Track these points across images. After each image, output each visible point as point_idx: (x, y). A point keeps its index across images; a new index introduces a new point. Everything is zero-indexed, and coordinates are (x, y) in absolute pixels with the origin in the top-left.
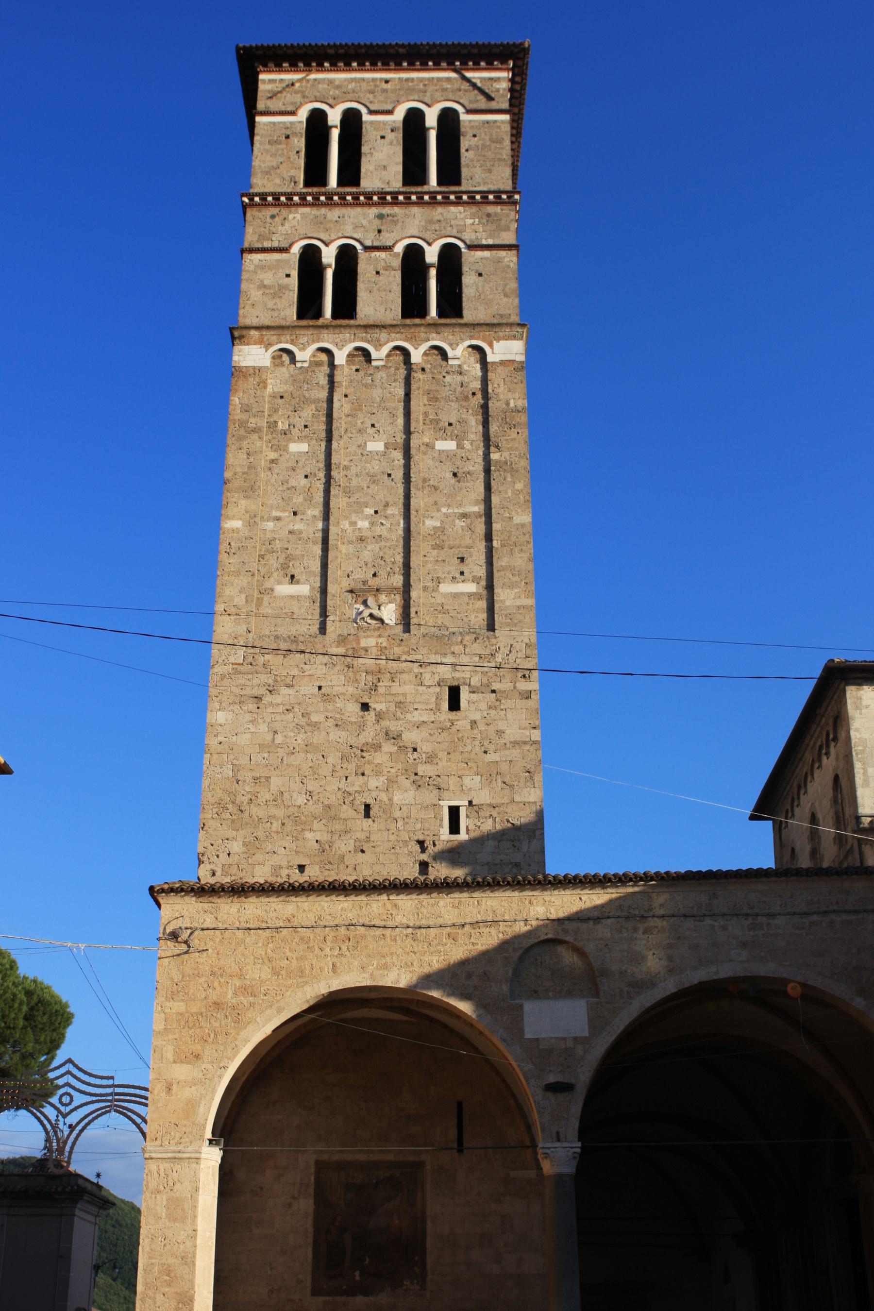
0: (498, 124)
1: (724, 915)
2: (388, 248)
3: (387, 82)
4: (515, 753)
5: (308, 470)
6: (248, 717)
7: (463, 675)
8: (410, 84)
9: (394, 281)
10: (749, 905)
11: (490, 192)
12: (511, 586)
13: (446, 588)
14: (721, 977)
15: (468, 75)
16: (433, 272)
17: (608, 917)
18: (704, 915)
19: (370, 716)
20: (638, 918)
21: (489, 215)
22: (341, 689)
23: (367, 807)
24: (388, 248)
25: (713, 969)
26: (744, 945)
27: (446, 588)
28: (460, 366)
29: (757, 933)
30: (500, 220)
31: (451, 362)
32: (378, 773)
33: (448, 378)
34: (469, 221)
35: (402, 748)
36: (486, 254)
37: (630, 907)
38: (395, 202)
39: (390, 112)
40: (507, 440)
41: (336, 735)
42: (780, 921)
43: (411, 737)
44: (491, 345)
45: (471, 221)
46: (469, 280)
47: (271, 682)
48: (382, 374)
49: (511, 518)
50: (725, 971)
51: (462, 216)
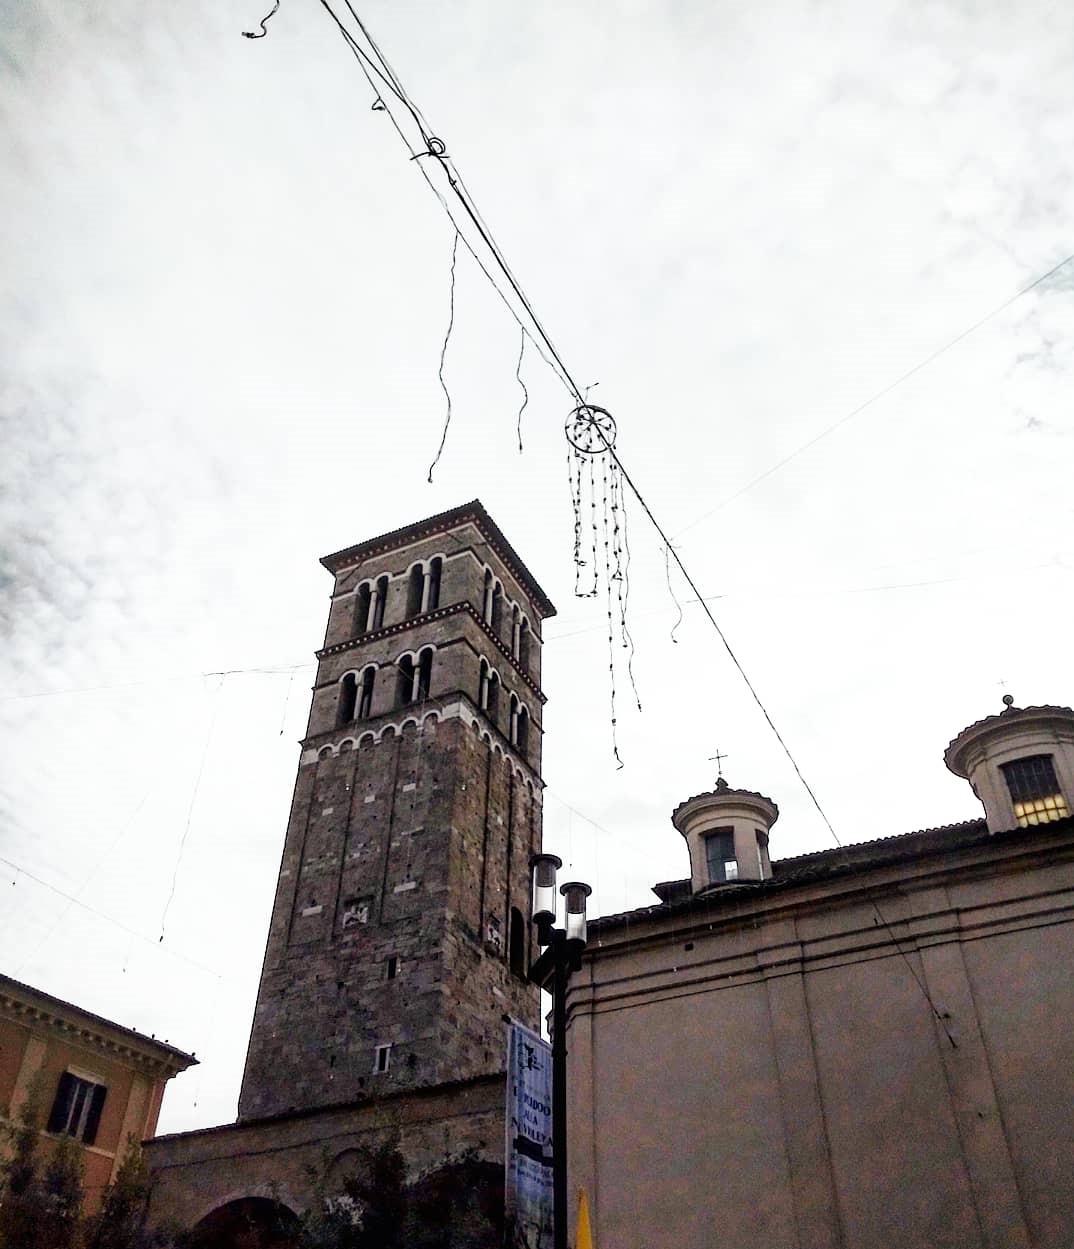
2: (390, 663)
3: (404, 552)
4: (424, 1002)
5: (331, 826)
6: (275, 1006)
7: (399, 950)
9: (392, 685)
11: (450, 607)
12: (434, 879)
13: (397, 890)
15: (449, 532)
16: (417, 670)
19: (344, 990)
21: (450, 623)
22: (328, 976)
23: (333, 1058)
24: (390, 663)
27: (397, 890)
32: (341, 1032)
35: (358, 1011)
36: (446, 649)
38: (399, 631)
39: (404, 572)
41: (323, 1009)
43: (364, 1002)
44: (441, 711)
46: (435, 669)
47: (291, 977)
48: (379, 748)
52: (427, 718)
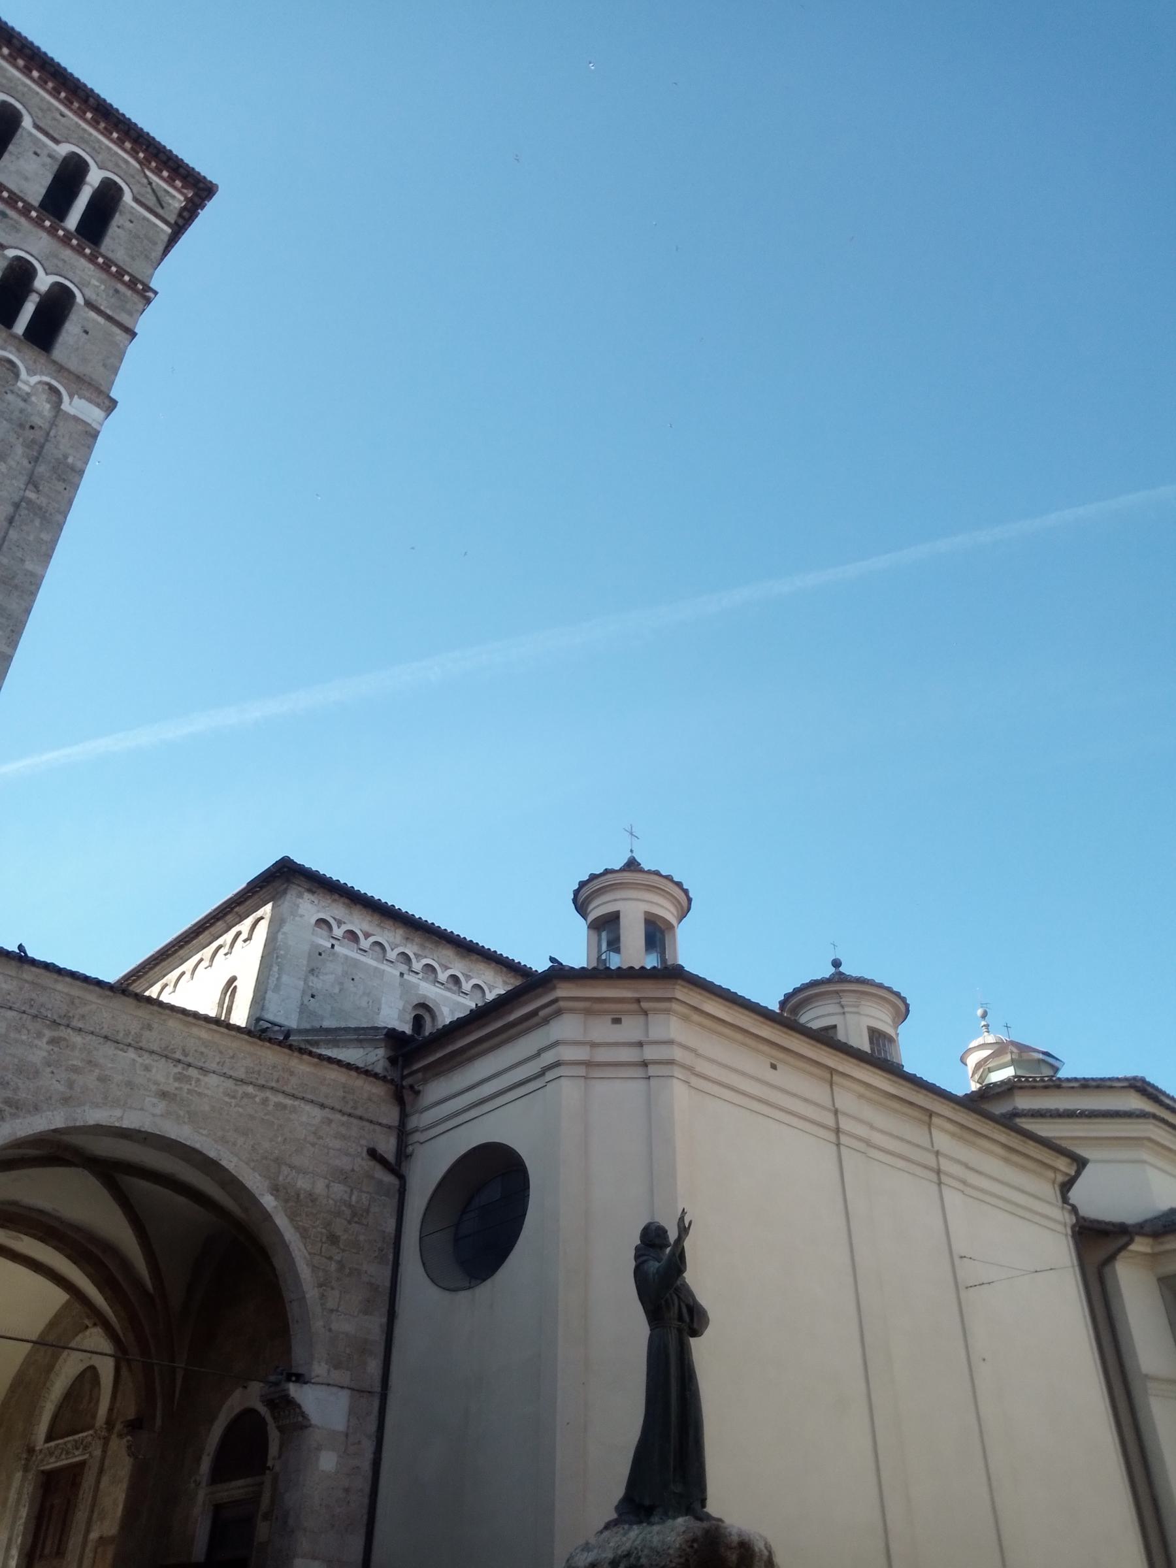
0: (158, 230)
1: (152, 1052)
3: (63, 115)
8: (86, 136)
10: (184, 1050)
14: (124, 1126)
17: (10, 1008)
18: (129, 1045)
20: (48, 1022)
21: (117, 291)
25: (118, 1113)
26: (164, 1095)
28: (28, 394)
29: (182, 1085)
30: (126, 302)
31: (20, 384)
33: (10, 397)
34: (94, 282)
37: (42, 1005)
38: (25, 212)
40: (50, 488)
42: (213, 1080)
45: (97, 284)
49: (22, 561)
50: (131, 1121)
51: (89, 273)
52: (40, 382)
